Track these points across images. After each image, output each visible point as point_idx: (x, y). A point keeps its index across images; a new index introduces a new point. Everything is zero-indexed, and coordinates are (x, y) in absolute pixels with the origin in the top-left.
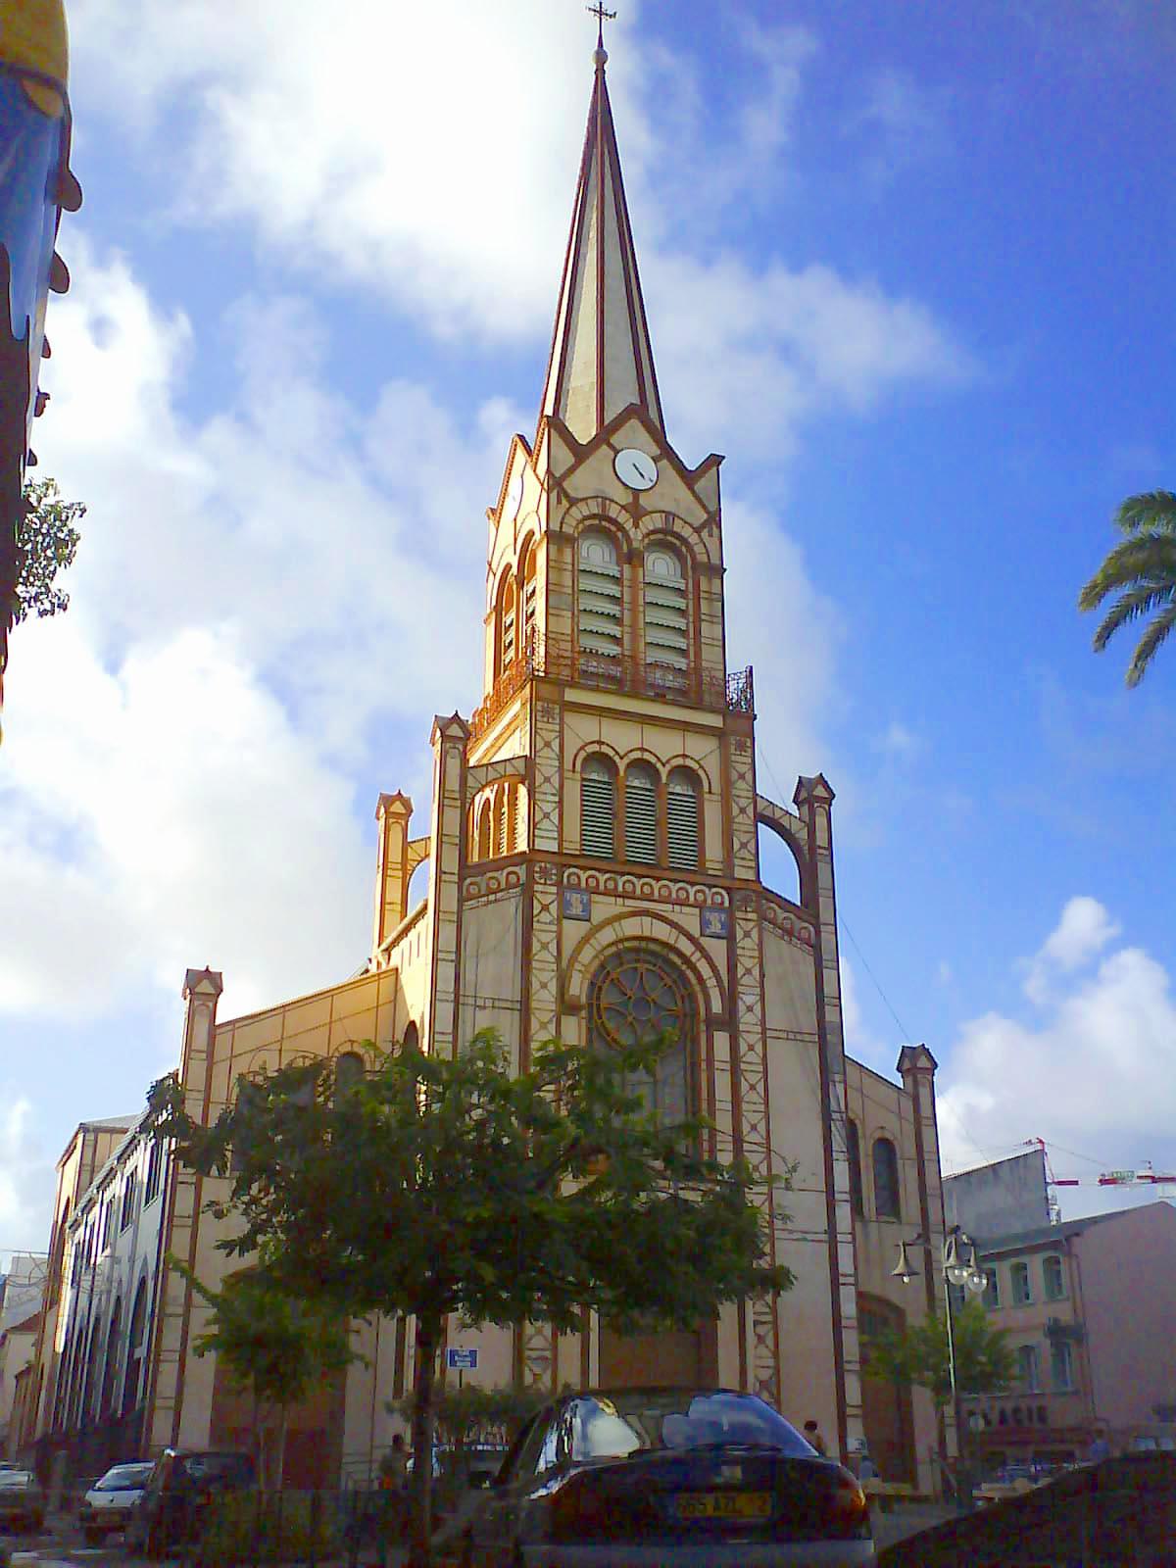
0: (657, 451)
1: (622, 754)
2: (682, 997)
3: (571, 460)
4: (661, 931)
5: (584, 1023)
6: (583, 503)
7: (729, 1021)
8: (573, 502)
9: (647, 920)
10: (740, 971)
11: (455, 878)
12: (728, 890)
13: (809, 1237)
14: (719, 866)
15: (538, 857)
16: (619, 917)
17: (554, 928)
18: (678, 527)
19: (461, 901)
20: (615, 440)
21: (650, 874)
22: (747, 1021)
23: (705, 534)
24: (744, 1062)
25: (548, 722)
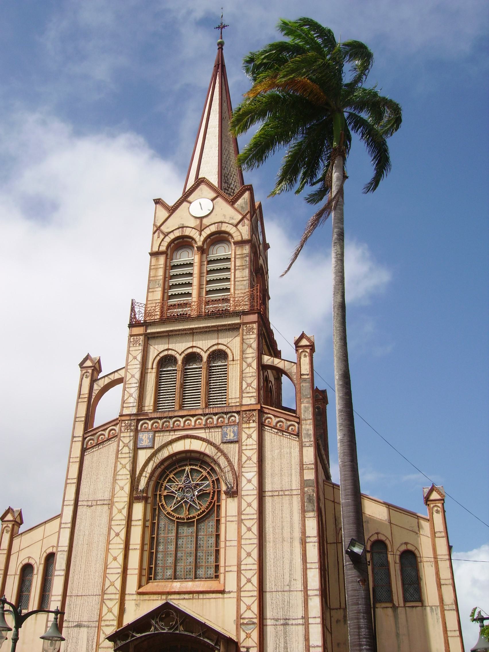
0: (213, 195)
2: (213, 482)
3: (167, 214)
4: (196, 446)
5: (149, 507)
6: (172, 233)
8: (166, 235)
9: (188, 441)
11: (81, 439)
12: (238, 412)
14: (238, 400)
18: (225, 228)
19: (84, 450)
20: (190, 199)
21: (189, 414)
23: (240, 226)
24: (244, 514)
25: (136, 346)
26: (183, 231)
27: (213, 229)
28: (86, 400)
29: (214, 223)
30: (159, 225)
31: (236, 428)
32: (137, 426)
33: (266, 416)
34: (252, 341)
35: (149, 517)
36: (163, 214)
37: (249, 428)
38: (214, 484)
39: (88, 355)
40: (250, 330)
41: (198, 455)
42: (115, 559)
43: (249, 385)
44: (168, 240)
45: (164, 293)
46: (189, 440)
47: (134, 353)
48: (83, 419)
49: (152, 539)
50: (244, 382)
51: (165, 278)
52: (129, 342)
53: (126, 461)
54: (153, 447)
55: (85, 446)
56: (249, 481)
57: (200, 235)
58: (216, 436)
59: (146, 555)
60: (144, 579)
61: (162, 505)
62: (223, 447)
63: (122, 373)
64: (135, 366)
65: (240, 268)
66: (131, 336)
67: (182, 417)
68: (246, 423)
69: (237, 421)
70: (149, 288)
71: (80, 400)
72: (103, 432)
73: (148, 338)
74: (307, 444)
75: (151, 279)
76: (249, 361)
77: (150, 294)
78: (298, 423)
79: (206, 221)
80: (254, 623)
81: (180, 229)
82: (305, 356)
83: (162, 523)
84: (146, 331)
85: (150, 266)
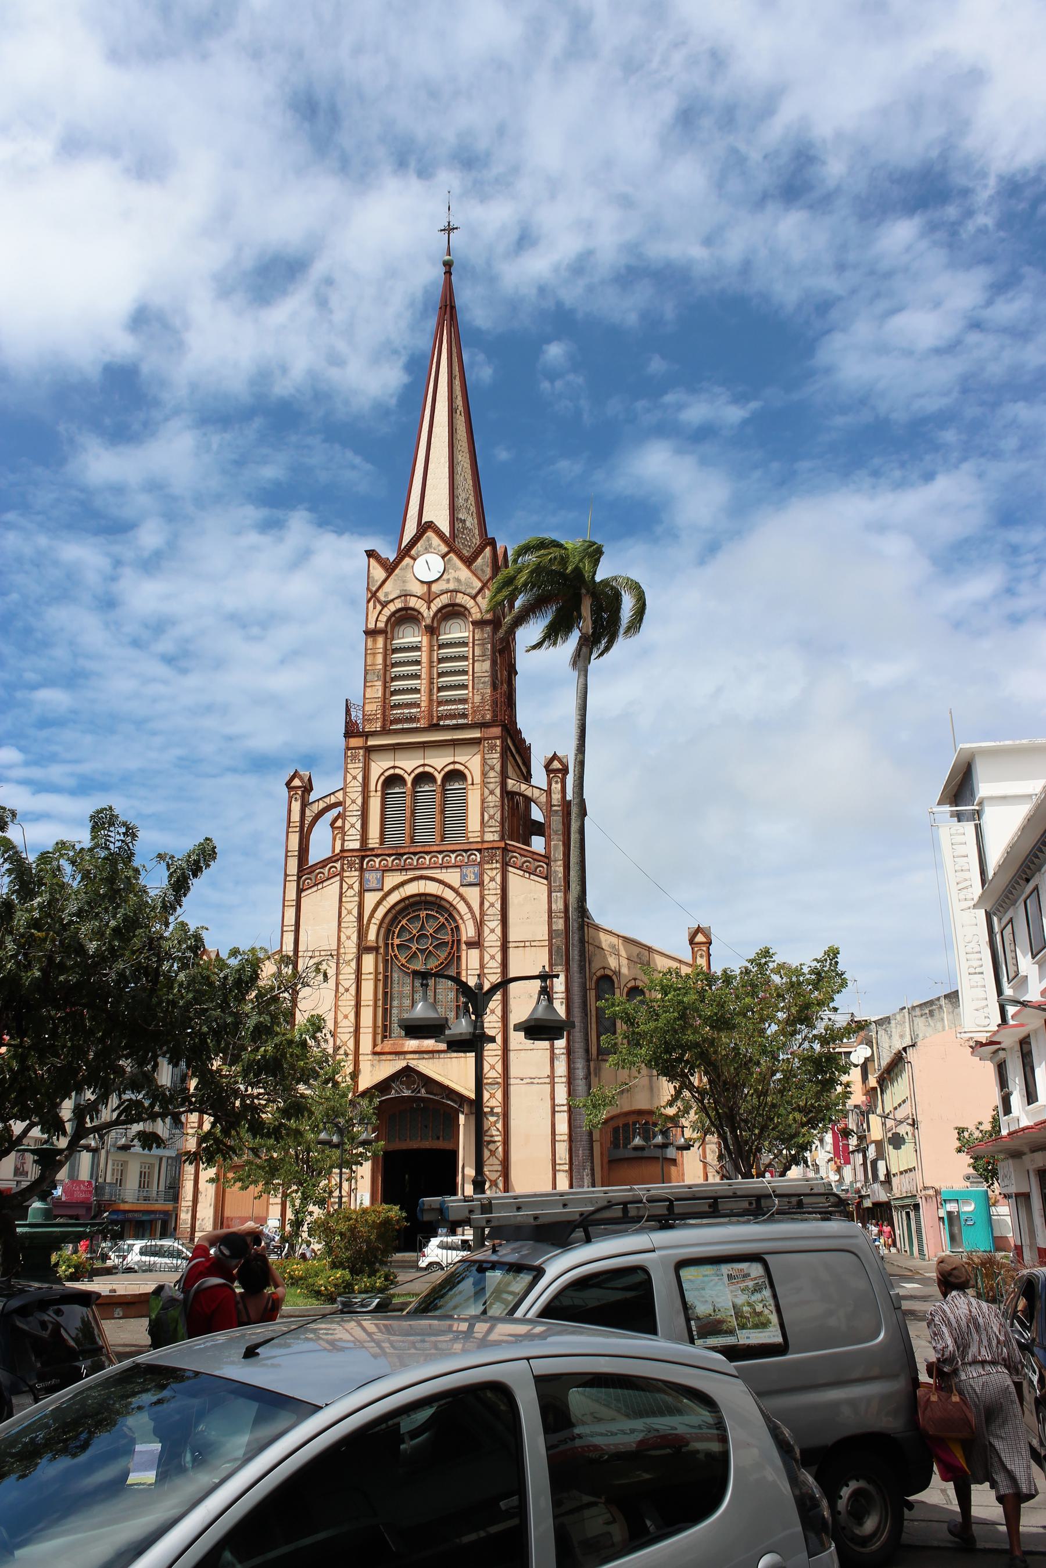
0: (444, 549)
1: (409, 772)
2: (452, 929)
4: (432, 888)
5: (380, 958)
6: (392, 604)
7: (476, 944)
8: (384, 605)
9: (422, 882)
10: (486, 904)
11: (295, 878)
12: (479, 850)
13: (536, 1081)
14: (479, 834)
15: (346, 854)
16: (402, 884)
17: (356, 899)
18: (460, 599)
19: (300, 891)
20: (413, 552)
22: (492, 939)
23: (479, 599)
26: (406, 601)
27: (444, 599)
28: (298, 829)
29: (447, 592)
30: (374, 589)
31: (476, 869)
32: (362, 864)
33: (511, 854)
34: (495, 761)
35: (381, 970)
36: (379, 573)
37: (492, 869)
38: (453, 932)
39: (296, 771)
40: (492, 748)
41: (433, 899)
42: (346, 1017)
43: (491, 817)
44: (387, 612)
45: (385, 687)
46: (424, 881)
47: (354, 772)
48: (296, 853)
49: (385, 994)
50: (485, 814)
51: (385, 666)
52: (346, 757)
53: (352, 906)
54: (382, 890)
55: (301, 887)
56: (492, 931)
57: (429, 608)
58: (453, 877)
59: (380, 1011)
60: (379, 1037)
61: (395, 955)
62: (462, 890)
63: (340, 795)
64: (356, 789)
65: (480, 658)
66: (348, 748)
67: (415, 854)
68: (489, 863)
69: (479, 860)
70: (365, 681)
71: (290, 830)
72: (322, 870)
73: (369, 751)
74: (557, 889)
75: (368, 668)
76: (491, 786)
77: (368, 690)
78: (547, 864)
79: (435, 588)
80: (498, 1083)
81: (403, 598)
82: (557, 782)
83: (395, 975)
84: (366, 743)
85: (366, 650)
